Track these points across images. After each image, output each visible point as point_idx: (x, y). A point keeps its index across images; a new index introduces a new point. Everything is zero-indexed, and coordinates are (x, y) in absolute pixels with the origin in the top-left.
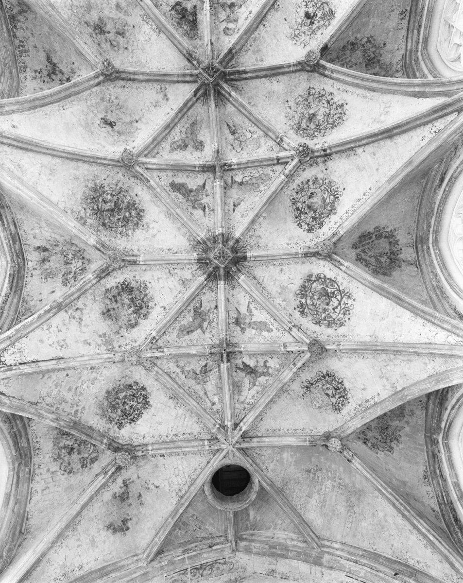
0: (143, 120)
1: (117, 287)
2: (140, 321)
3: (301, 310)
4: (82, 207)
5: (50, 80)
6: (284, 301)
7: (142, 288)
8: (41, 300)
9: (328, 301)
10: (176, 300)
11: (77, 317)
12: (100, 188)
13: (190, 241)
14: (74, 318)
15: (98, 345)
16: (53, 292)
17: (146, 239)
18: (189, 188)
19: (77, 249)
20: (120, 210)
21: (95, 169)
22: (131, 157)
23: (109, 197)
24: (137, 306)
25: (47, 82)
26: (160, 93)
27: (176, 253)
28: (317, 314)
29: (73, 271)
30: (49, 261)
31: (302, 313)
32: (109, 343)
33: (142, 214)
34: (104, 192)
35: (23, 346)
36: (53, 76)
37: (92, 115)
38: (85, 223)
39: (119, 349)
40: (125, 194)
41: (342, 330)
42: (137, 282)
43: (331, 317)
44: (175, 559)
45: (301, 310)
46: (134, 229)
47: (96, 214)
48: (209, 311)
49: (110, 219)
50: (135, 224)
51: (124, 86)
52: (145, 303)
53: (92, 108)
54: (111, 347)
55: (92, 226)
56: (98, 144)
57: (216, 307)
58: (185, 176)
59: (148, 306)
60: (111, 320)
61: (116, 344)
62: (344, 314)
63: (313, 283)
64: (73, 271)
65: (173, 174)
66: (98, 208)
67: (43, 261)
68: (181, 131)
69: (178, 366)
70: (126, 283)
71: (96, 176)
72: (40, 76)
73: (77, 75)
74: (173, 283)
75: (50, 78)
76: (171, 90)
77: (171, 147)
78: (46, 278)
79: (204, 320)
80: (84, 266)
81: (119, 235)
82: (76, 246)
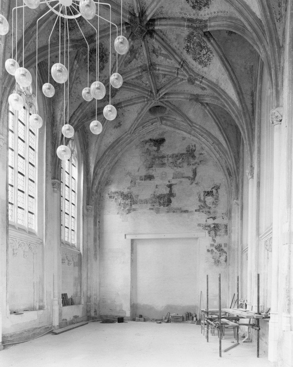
3: (187, 50)
6: (178, 44)
9: (201, 49)
28: (195, 54)
31: (188, 51)
41: (205, 69)
43: (201, 59)
44: (140, 132)
45: (187, 50)
48: (138, 48)
57: (141, 46)
62: (208, 60)
63: (194, 36)
79: (136, 53)
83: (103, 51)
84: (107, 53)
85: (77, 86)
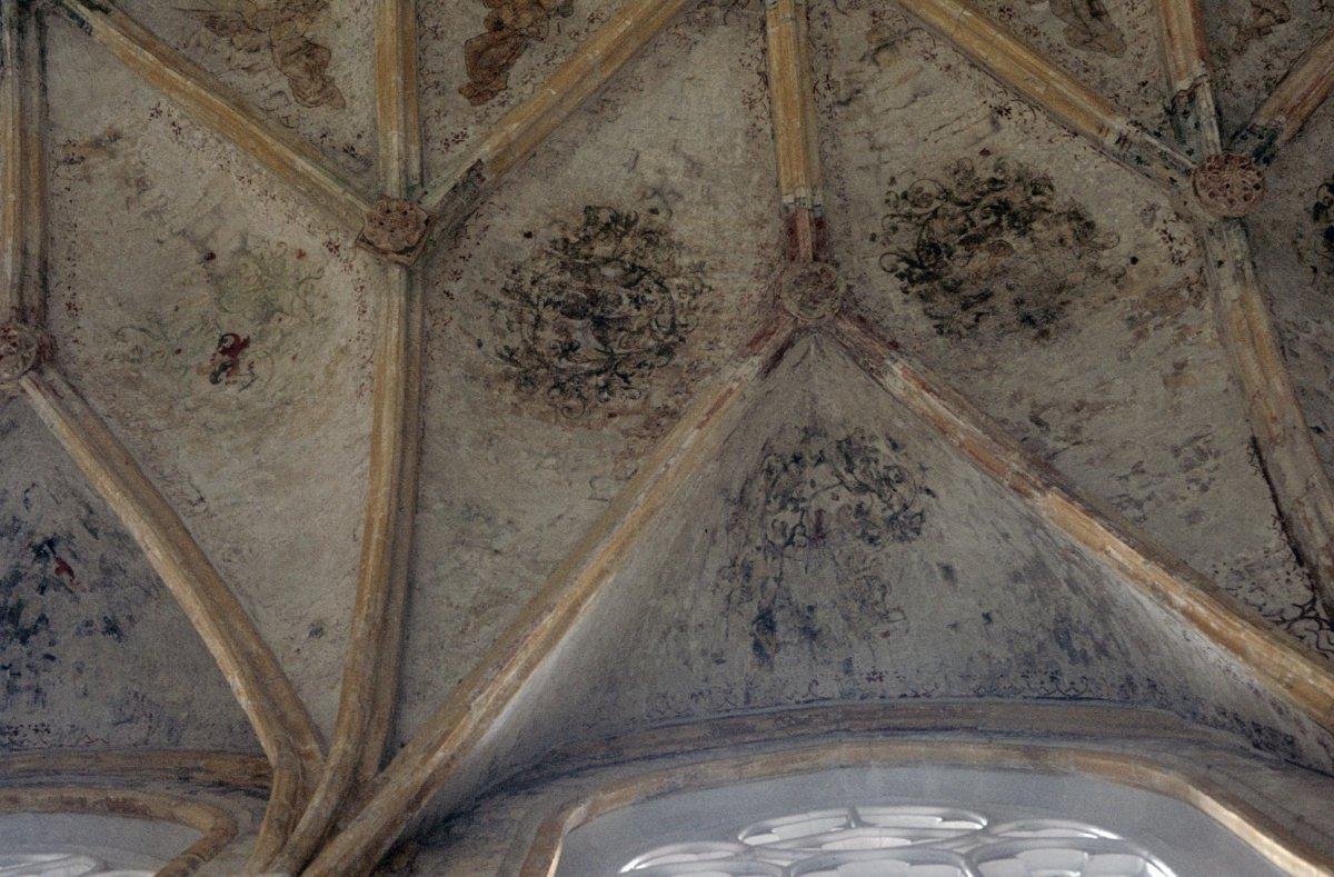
0: (202, 230)
1: (923, 297)
2: (1059, 202)
4: (605, 424)
5: (43, 634)
7: (917, 211)
8: (987, 617)
10: (965, 69)
11: (1072, 419)
12: (516, 363)
13: (709, 22)
14: (1077, 430)
15: (1182, 337)
16: (948, 571)
17: (710, 199)
18: (484, 30)
19: (762, 480)
20: (594, 299)
21: (445, 375)
22: (397, 216)
23: (549, 336)
24: (997, 224)
25: (52, 644)
26: (86, 168)
27: (765, 77)
29: (854, 499)
30: (811, 609)
32: (1165, 302)
33: (604, 216)
34: (530, 351)
35: (1220, 567)
36: (28, 618)
37: (207, 412)
38: (666, 412)
39: (1190, 262)
40: (528, 276)
42: (895, 229)
46: (671, 244)
47: (624, 377)
49: (640, 331)
50: (649, 241)
51: (69, 306)
52: (982, 194)
53: (178, 412)
54: (1184, 293)
55: (682, 389)
56: (330, 374)
58: (438, 46)
59: (994, 181)
60: (1067, 309)
61: (1171, 275)
64: (854, 499)
65: (432, 91)
66: (599, 373)
67: (811, 634)
68: (248, 69)
69: (1240, 51)
70: (903, 266)
71: (472, 374)
72: (26, 673)
73: (22, 514)
74: (888, 86)
75: (35, 630)
76: (78, 123)
77: (316, 103)
78: (885, 616)
80: (831, 453)
81: (703, 300)
82: (749, 481)
83: (965, 198)
84: (989, 174)
85: (1101, 442)
